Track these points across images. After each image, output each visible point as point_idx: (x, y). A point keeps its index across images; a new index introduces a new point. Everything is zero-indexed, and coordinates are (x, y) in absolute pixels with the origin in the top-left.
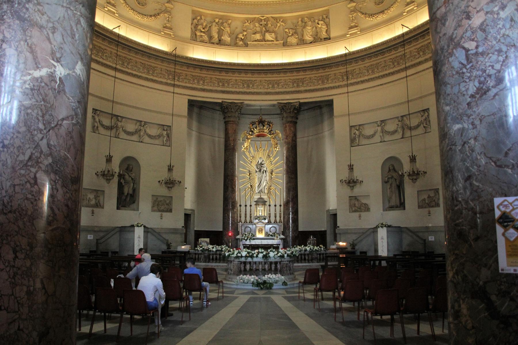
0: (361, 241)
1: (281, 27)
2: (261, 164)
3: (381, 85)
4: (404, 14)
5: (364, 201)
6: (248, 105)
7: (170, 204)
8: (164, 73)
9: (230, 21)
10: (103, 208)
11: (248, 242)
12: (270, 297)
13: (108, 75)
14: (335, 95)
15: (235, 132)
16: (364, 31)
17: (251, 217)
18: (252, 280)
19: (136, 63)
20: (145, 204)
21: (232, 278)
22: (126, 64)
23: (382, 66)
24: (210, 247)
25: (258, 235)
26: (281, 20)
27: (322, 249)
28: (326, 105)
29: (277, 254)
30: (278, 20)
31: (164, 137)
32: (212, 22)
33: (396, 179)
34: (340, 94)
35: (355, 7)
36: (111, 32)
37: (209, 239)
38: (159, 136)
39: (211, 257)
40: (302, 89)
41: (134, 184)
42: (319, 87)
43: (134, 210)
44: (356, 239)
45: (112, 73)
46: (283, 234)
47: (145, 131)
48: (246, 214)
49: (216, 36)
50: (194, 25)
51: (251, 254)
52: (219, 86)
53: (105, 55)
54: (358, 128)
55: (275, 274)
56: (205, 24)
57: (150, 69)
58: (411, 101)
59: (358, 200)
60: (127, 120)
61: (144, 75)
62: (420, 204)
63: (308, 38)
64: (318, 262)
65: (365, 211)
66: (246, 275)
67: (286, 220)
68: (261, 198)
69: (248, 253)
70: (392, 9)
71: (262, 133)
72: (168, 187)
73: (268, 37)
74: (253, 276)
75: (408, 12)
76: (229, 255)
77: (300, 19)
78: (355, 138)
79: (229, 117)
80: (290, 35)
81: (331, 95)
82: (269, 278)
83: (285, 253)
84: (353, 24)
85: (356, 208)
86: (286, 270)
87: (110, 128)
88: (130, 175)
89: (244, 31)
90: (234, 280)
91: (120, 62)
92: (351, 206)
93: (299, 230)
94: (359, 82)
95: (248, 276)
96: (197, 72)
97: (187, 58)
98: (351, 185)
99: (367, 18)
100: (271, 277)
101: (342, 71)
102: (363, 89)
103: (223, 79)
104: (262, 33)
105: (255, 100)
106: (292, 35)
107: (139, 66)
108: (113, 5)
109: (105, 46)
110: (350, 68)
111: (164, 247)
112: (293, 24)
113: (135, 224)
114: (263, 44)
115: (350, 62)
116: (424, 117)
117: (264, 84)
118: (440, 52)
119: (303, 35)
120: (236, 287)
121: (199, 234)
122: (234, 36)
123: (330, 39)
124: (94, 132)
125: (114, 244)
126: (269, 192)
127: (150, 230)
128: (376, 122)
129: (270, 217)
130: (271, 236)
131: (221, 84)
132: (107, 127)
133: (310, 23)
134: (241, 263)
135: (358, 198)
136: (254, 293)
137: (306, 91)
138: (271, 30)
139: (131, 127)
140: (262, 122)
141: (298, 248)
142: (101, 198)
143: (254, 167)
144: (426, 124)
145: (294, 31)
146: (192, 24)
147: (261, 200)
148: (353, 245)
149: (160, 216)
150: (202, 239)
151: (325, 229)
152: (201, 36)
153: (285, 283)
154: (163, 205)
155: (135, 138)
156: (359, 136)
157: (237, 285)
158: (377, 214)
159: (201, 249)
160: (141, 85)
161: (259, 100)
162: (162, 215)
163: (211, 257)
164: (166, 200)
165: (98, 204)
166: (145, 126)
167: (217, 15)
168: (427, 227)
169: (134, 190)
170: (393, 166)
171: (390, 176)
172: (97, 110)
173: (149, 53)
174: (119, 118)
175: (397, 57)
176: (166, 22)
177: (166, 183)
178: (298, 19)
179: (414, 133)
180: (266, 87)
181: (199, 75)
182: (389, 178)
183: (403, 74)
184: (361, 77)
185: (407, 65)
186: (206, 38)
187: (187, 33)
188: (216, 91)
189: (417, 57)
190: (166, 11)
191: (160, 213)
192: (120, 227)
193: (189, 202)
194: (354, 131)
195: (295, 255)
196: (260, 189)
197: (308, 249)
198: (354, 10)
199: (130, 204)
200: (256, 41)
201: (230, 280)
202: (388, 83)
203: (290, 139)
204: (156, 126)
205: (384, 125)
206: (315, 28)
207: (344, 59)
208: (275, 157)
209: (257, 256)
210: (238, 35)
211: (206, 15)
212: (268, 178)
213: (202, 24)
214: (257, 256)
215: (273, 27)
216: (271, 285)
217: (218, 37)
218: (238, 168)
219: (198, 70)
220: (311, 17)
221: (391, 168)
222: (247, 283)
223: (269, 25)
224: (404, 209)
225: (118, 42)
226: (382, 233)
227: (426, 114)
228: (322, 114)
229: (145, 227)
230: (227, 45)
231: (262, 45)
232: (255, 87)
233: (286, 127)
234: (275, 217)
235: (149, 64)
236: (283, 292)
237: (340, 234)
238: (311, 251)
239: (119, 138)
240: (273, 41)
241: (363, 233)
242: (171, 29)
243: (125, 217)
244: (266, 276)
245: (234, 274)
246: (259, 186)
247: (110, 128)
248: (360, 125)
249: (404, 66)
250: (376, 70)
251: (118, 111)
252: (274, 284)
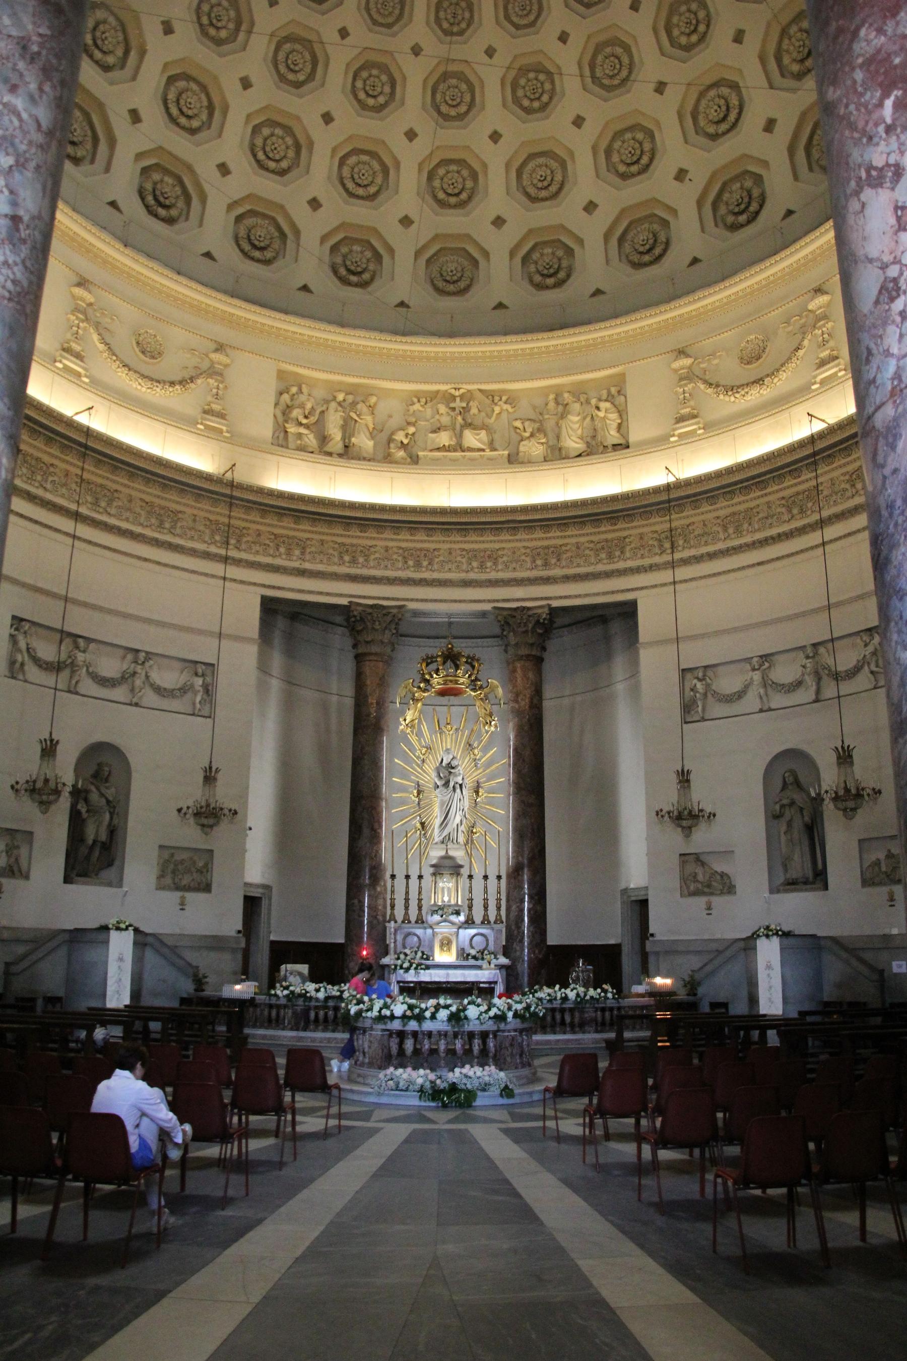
0: (713, 973)
1: (504, 416)
2: (450, 766)
3: (759, 564)
4: (814, 387)
5: (719, 867)
6: (416, 613)
7: (207, 869)
8: (202, 528)
9: (373, 400)
10: (27, 877)
11: (411, 976)
12: (466, 1130)
13: (57, 530)
14: (642, 588)
15: (383, 683)
16: (715, 427)
17: (420, 908)
18: (420, 1081)
19: (130, 501)
20: (139, 866)
21: (364, 1077)
22: (103, 504)
23: (761, 515)
24: (311, 987)
25: (441, 957)
26: (504, 398)
27: (610, 995)
28: (619, 614)
29: (486, 1012)
30: (497, 399)
31: (196, 693)
32: (327, 402)
33: (801, 809)
34: (655, 586)
35: (690, 368)
36: (70, 423)
37: (307, 966)
38: (184, 690)
39: (312, 1015)
40: (557, 572)
41: (112, 814)
42: (600, 568)
43: (110, 884)
44: (702, 968)
45: (67, 525)
46: (505, 955)
47: (147, 677)
48: (407, 900)
49: (336, 435)
50: (282, 406)
51: (417, 1011)
52: (342, 563)
53: (50, 479)
54: (700, 675)
55: (482, 1065)
56: (309, 406)
57: (164, 517)
58: (839, 604)
59: (703, 864)
60: (101, 646)
61: (148, 532)
62: (868, 875)
63: (573, 443)
64: (597, 1031)
65: (722, 893)
66: (403, 1066)
67: (513, 915)
68: (447, 857)
69: (411, 1007)
70: (783, 375)
71: (451, 685)
72: (203, 826)
73: (471, 439)
74: (421, 1072)
75: (822, 382)
76: (359, 1013)
77: (552, 397)
78: (694, 701)
79: (367, 642)
80: (527, 434)
81: (632, 590)
82: (466, 1076)
83: (510, 1009)
84: (686, 411)
85: (700, 886)
86: (512, 1055)
87: (56, 668)
88: (103, 790)
89: (409, 424)
90: (369, 1081)
91: (89, 499)
92: (684, 880)
93: (549, 943)
94: (702, 556)
95: (409, 1070)
96: (285, 527)
97: (261, 491)
98: (684, 823)
99: (721, 397)
100: (471, 1073)
101: (657, 528)
102: (714, 575)
103: (352, 545)
104: (454, 429)
105: (436, 601)
106: (532, 435)
107: (138, 510)
108: (78, 356)
109: (52, 456)
110: (679, 520)
111: (187, 987)
112: (534, 408)
113: (112, 922)
114: (456, 458)
115: (679, 505)
116: (870, 648)
117: (459, 559)
118: (885, 513)
119: (558, 438)
120: (372, 1099)
121: (283, 952)
122: (384, 436)
123: (628, 447)
124: (13, 677)
125: (50, 977)
126: (469, 841)
127: (150, 940)
128: (748, 660)
129: (470, 907)
130: (475, 958)
131: (347, 558)
132: (47, 663)
133: (577, 406)
134: (391, 1033)
135: (702, 857)
136: (424, 1119)
137: (567, 579)
138: (478, 422)
139: (110, 666)
140: (451, 658)
141: (544, 993)
142: (24, 851)
143: (429, 776)
144: (877, 666)
145: (537, 425)
146: (276, 404)
147: (447, 863)
148: (692, 985)
149: (178, 901)
150: (289, 966)
151: (619, 941)
152: (299, 436)
153: (507, 1092)
154: (187, 872)
155: (120, 693)
156: (705, 695)
157: (379, 1094)
158: (754, 902)
159: (286, 992)
160: (139, 558)
161: (445, 601)
162: (183, 898)
163: (312, 1015)
164: (195, 858)
165: (15, 869)
166: (147, 664)
167: (340, 383)
168: (887, 937)
169: (112, 831)
170: (793, 773)
171: (785, 802)
172: (22, 620)
173: (163, 477)
174: (80, 641)
175: (798, 494)
176: (209, 398)
177: (197, 815)
178: (547, 396)
179: (846, 687)
180: (464, 567)
181: (291, 533)
182: (783, 806)
183: (814, 538)
184: (706, 544)
185: (825, 513)
186: (311, 439)
187: (264, 428)
188: (335, 577)
189: (849, 494)
190: (213, 372)
192: (70, 931)
193: (256, 864)
194: (691, 681)
195: (535, 1014)
196: (445, 833)
197: (572, 995)
198: (688, 376)
199: (101, 869)
200: (438, 449)
201: (360, 1080)
202: (778, 559)
203: (524, 703)
204: (178, 665)
205: (770, 667)
206: (588, 419)
207: (664, 497)
208: (485, 750)
209: (433, 1017)
210: (393, 434)
211: (313, 383)
212: (466, 804)
213: (302, 406)
214: (433, 1017)
215: (483, 414)
216: (470, 1095)
217: (343, 438)
218: (391, 774)
219: (287, 522)
220: (579, 392)
221: (790, 780)
222: (407, 1090)
223: (474, 411)
224: (826, 887)
225: (86, 447)
226: (769, 953)
227: (877, 639)
228: (607, 639)
229: (136, 930)
230: (364, 459)
231: (454, 461)
232: (436, 567)
233: (514, 671)
234: (486, 908)
235: (163, 503)
236: (503, 1115)
237: (657, 954)
238: (581, 1001)
239: (77, 693)
240: (483, 450)
241: (719, 952)
242: (221, 416)
243: (86, 904)
244: (457, 1070)
245: (371, 1065)
246: (444, 824)
247: (56, 668)
248: (706, 667)
249: (816, 517)
250: (746, 526)
251: (79, 622)
252: (479, 1093)
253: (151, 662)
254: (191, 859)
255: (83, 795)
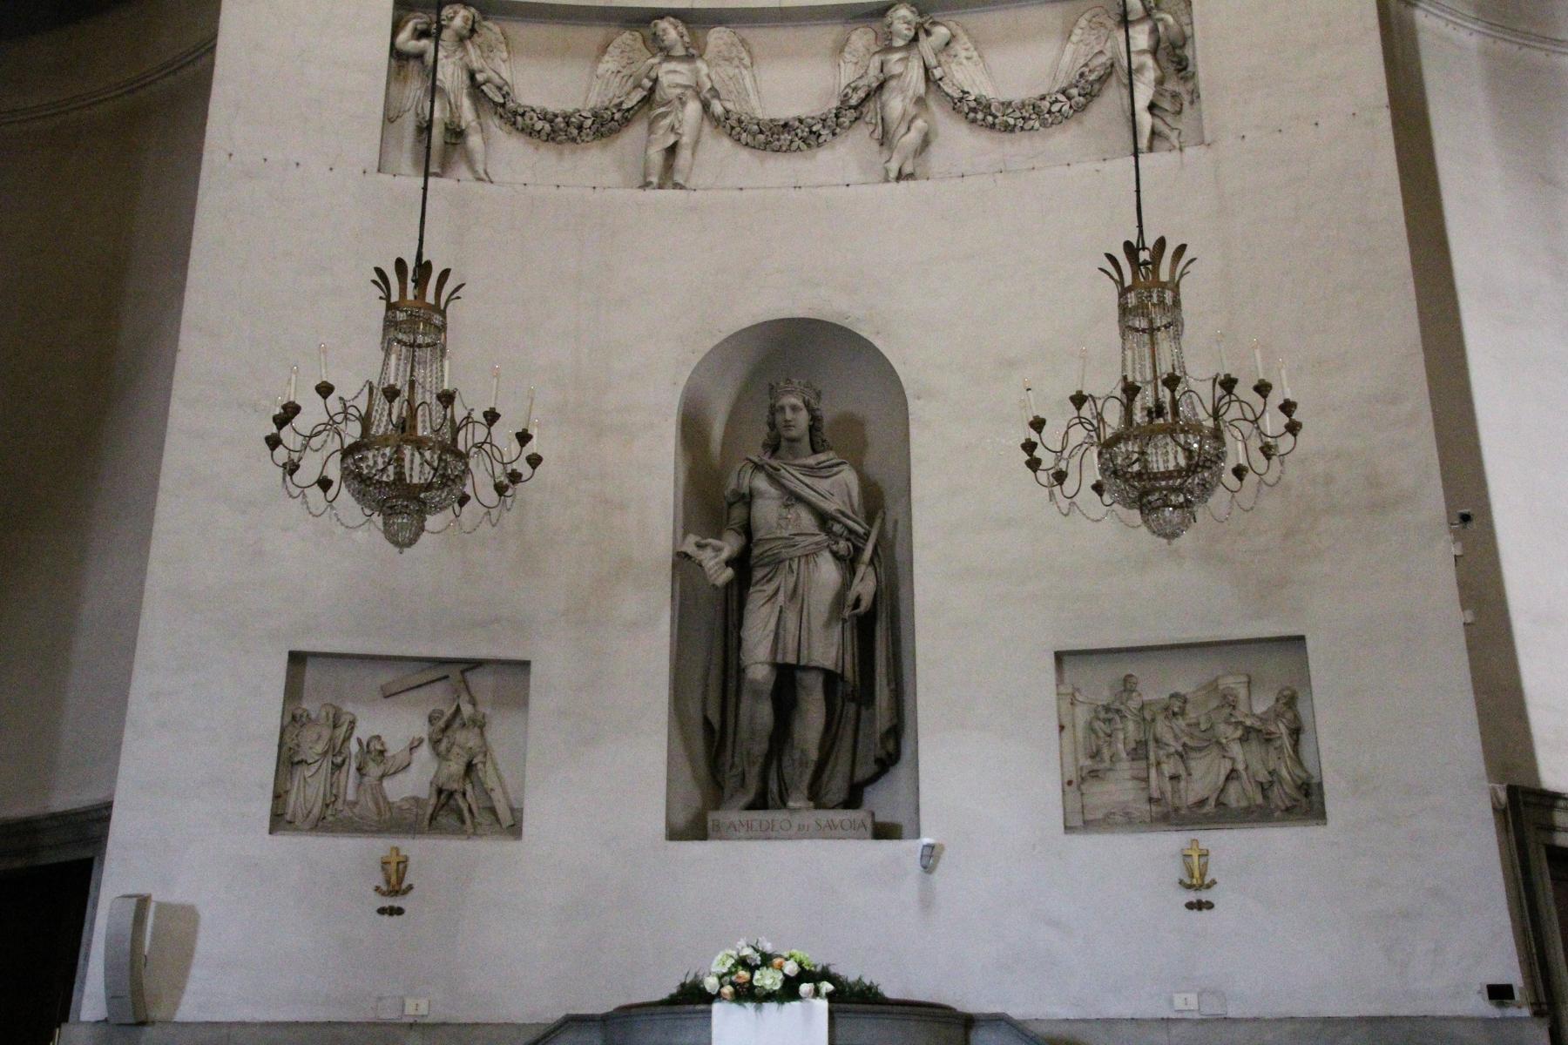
7: (1290, 723)
20: (983, 750)
38: (1085, 92)
41: (849, 564)
88: (794, 479)
142: (500, 732)
149: (1176, 871)
155: (847, 156)
164: (1234, 683)
166: (926, 45)
191: (1172, 841)
253: (941, 32)
254: (1212, 687)
255: (738, 513)
